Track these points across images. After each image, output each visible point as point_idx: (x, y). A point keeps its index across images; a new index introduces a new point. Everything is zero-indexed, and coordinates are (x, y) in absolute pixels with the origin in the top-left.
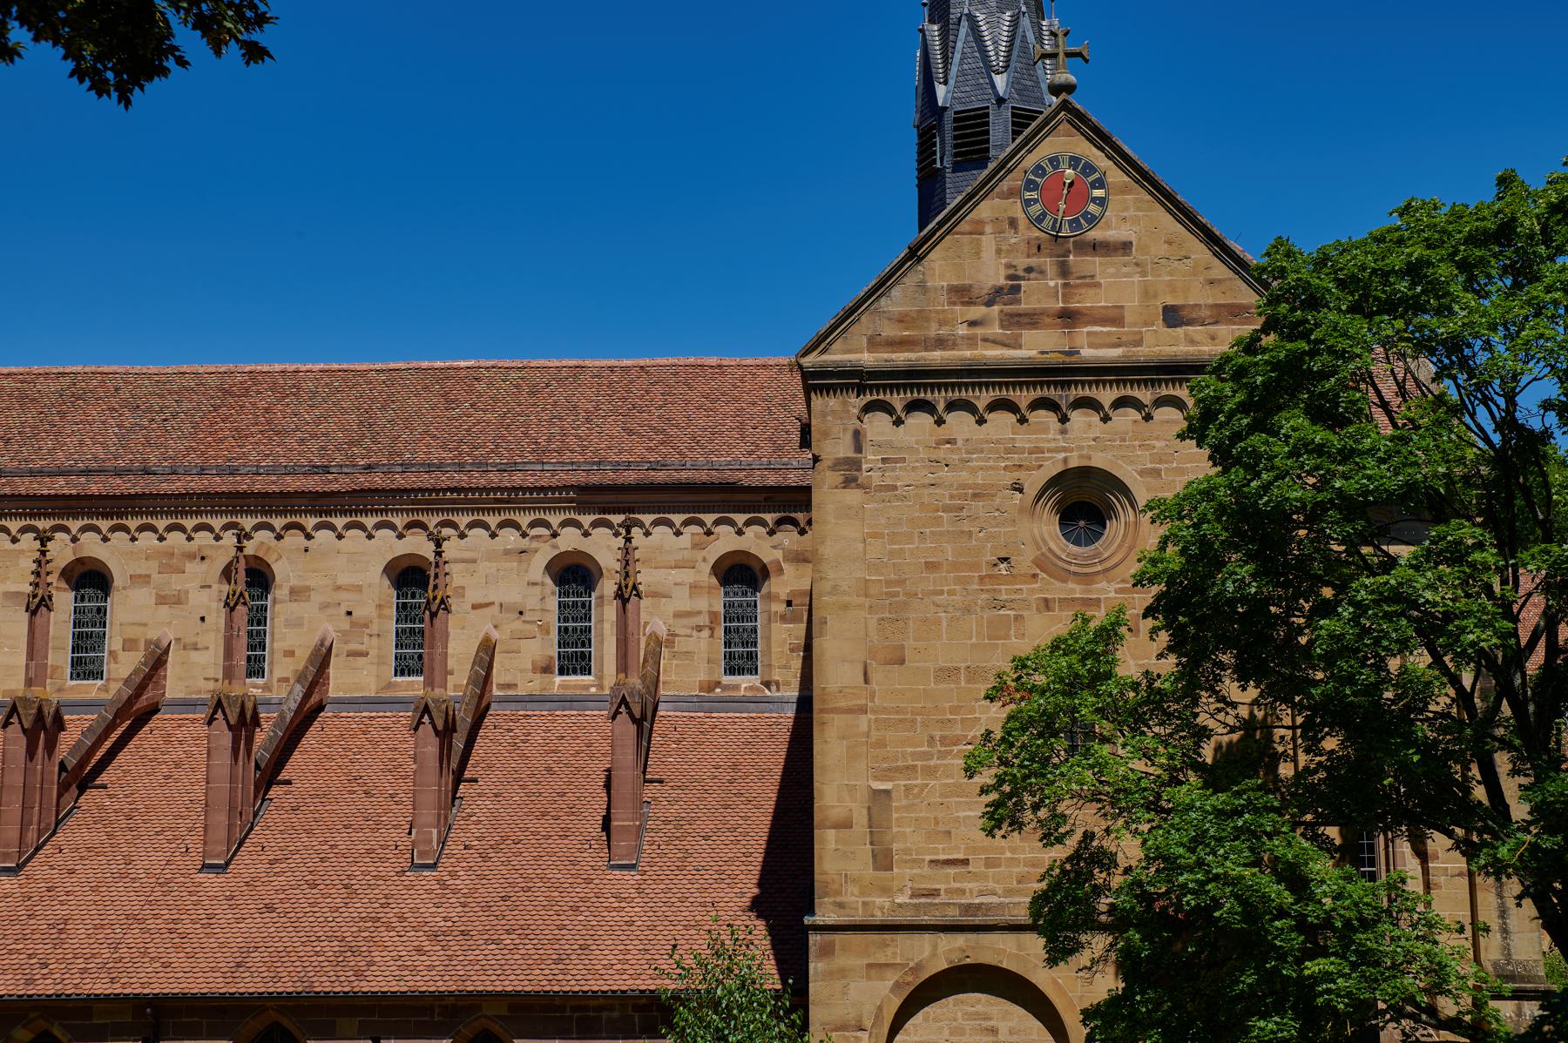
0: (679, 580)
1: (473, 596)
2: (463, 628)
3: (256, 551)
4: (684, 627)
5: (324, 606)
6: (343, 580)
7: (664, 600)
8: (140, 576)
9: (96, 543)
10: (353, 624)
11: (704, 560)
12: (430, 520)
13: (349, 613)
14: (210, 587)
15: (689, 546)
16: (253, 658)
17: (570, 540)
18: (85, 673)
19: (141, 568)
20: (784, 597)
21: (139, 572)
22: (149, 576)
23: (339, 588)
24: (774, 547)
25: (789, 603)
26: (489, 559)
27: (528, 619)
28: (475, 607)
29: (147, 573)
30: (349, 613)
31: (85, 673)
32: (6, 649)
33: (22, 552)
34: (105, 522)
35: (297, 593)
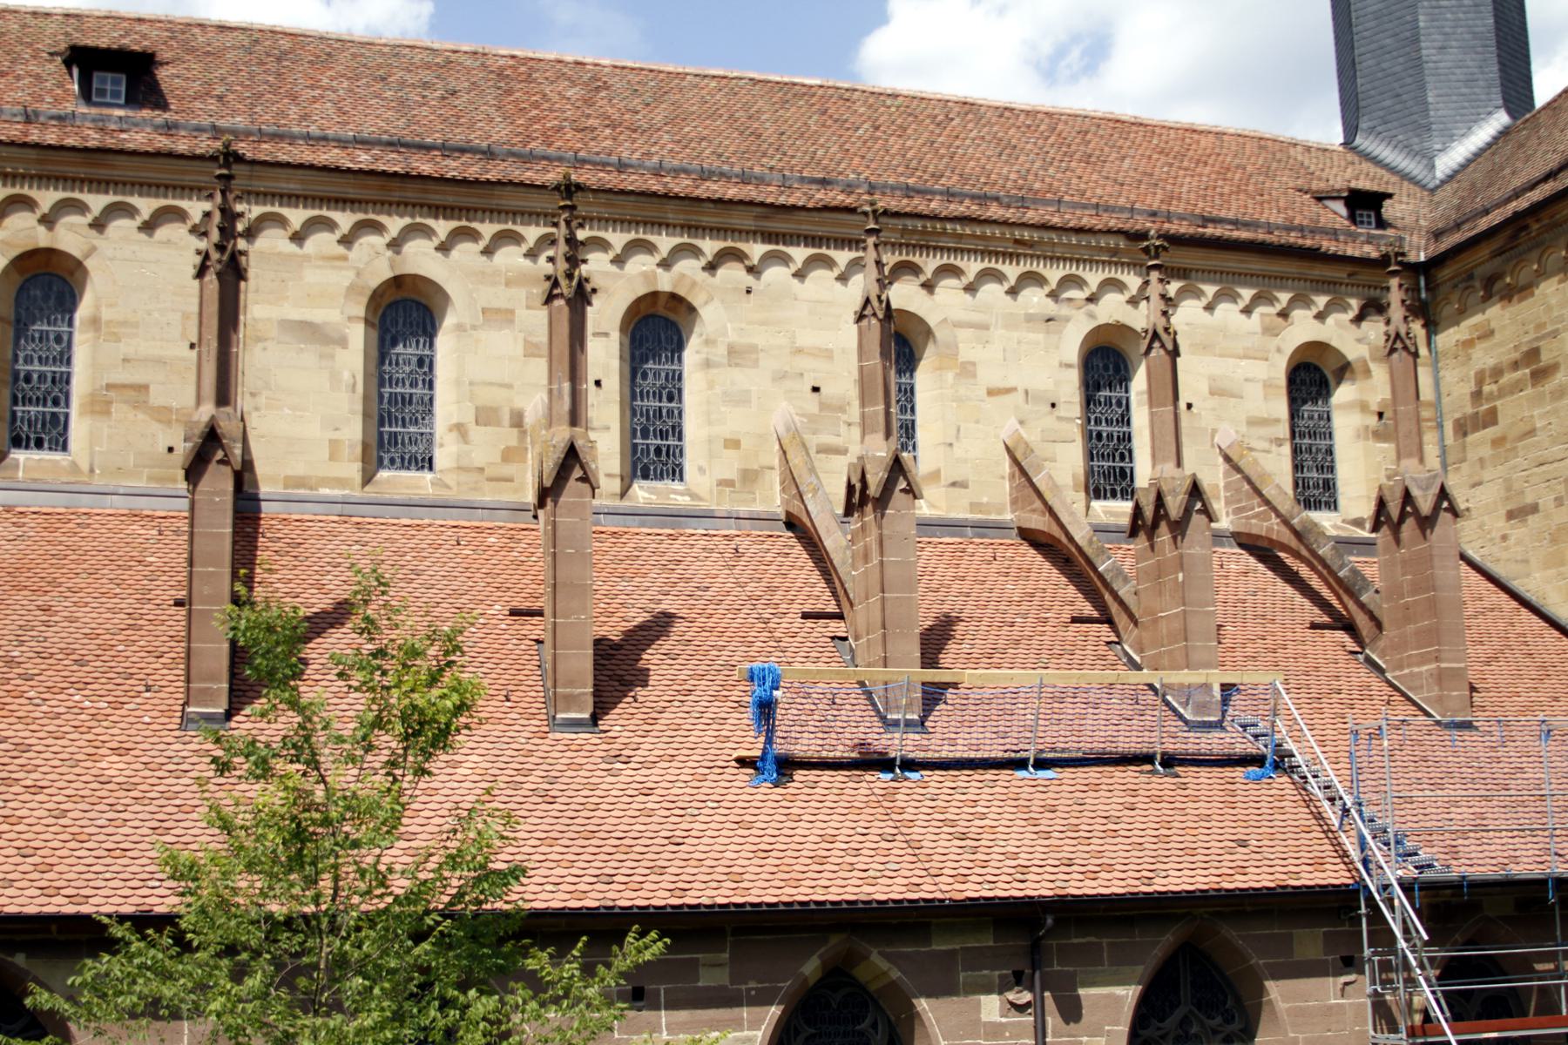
0: (1250, 375)
1: (990, 376)
2: (977, 422)
3: (675, 286)
4: (1260, 438)
5: (779, 377)
6: (806, 339)
7: (1233, 400)
8: (498, 311)
9: (425, 254)
10: (823, 406)
11: (1279, 350)
12: (926, 263)
13: (816, 389)
14: (606, 334)
15: (1259, 330)
16: (664, 449)
17: (1113, 309)
18: (403, 459)
19: (499, 297)
20: (1375, 408)
21: (496, 304)
22: (512, 312)
23: (799, 351)
24: (1359, 341)
25: (1380, 415)
26: (1007, 327)
27: (1062, 414)
28: (991, 392)
29: (509, 306)
30: (816, 389)
31: (403, 459)
32: (287, 411)
33: (307, 258)
34: (441, 222)
35: (738, 355)
